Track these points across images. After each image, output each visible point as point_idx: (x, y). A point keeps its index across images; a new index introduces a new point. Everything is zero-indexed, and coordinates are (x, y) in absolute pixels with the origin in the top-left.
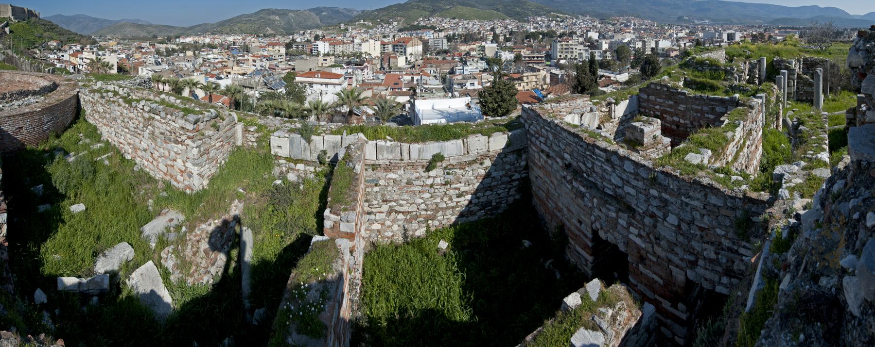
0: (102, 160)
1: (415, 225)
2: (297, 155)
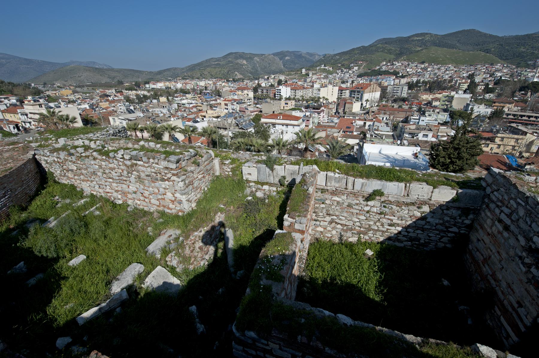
1: (349, 234)
2: (263, 179)
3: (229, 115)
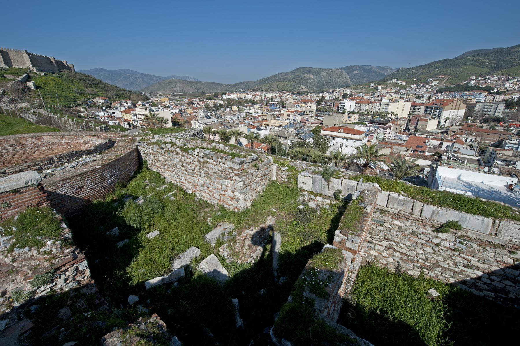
0: (169, 197)
1: (409, 266)
2: (317, 190)
3: (290, 125)
